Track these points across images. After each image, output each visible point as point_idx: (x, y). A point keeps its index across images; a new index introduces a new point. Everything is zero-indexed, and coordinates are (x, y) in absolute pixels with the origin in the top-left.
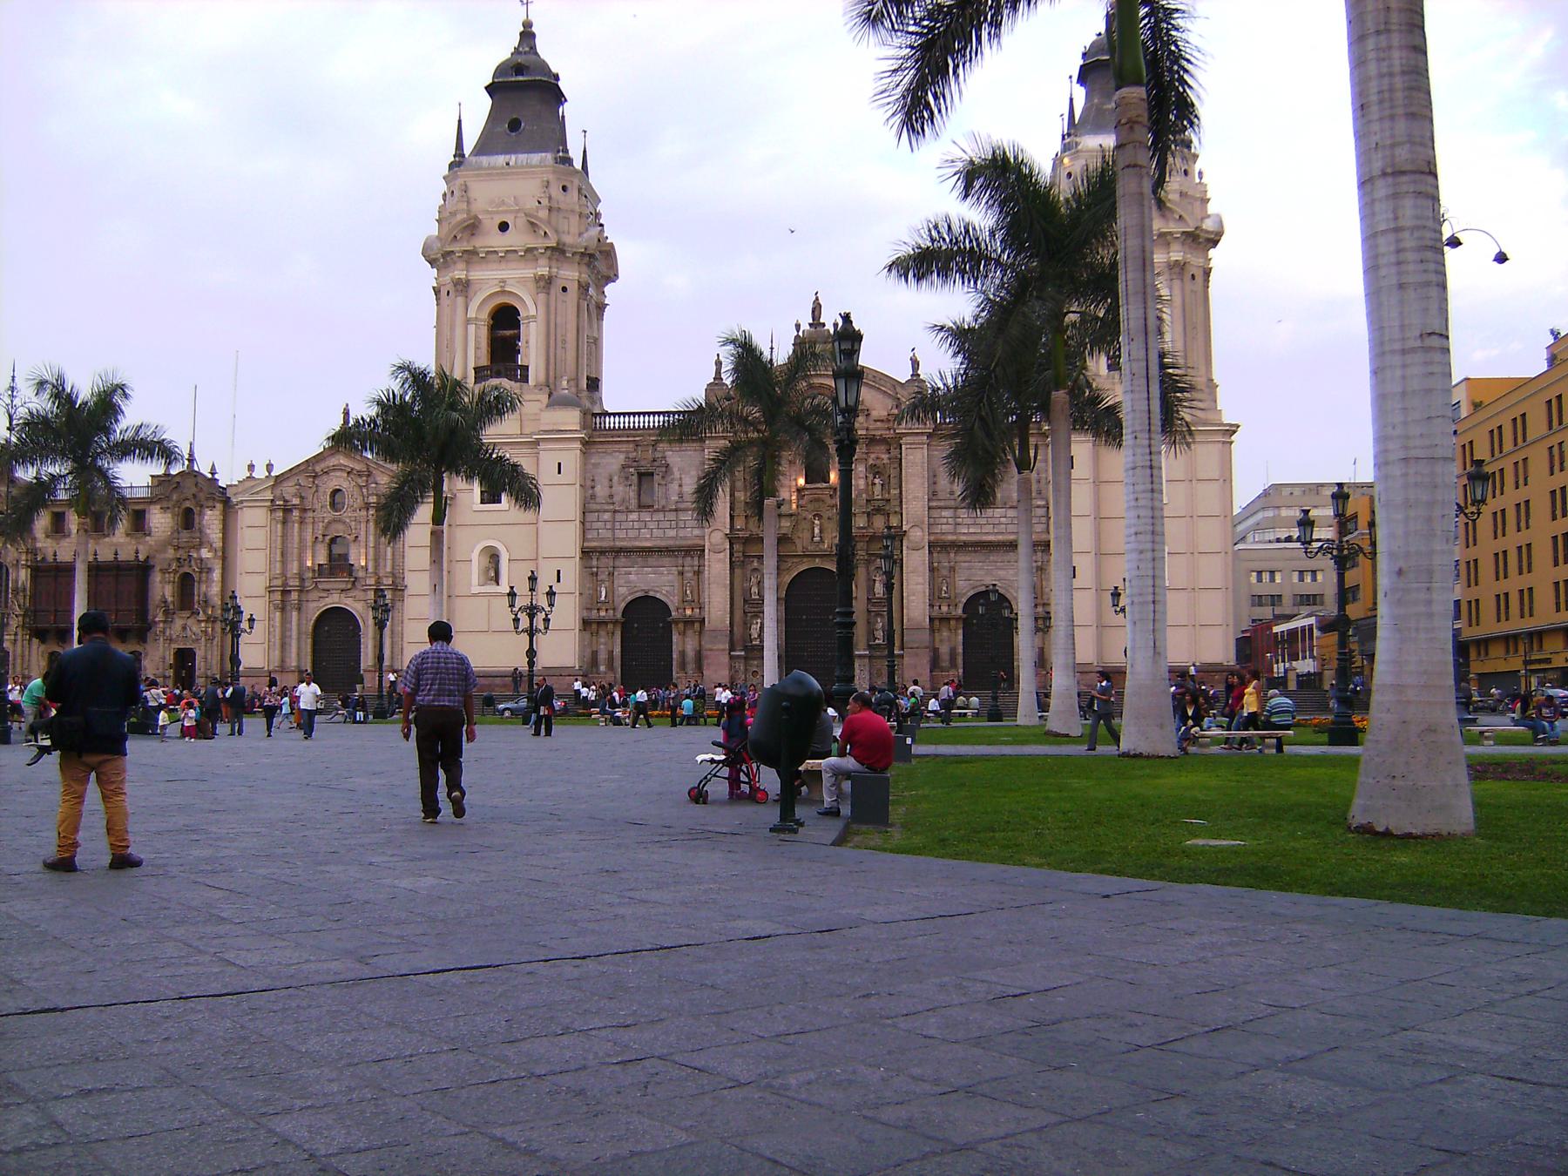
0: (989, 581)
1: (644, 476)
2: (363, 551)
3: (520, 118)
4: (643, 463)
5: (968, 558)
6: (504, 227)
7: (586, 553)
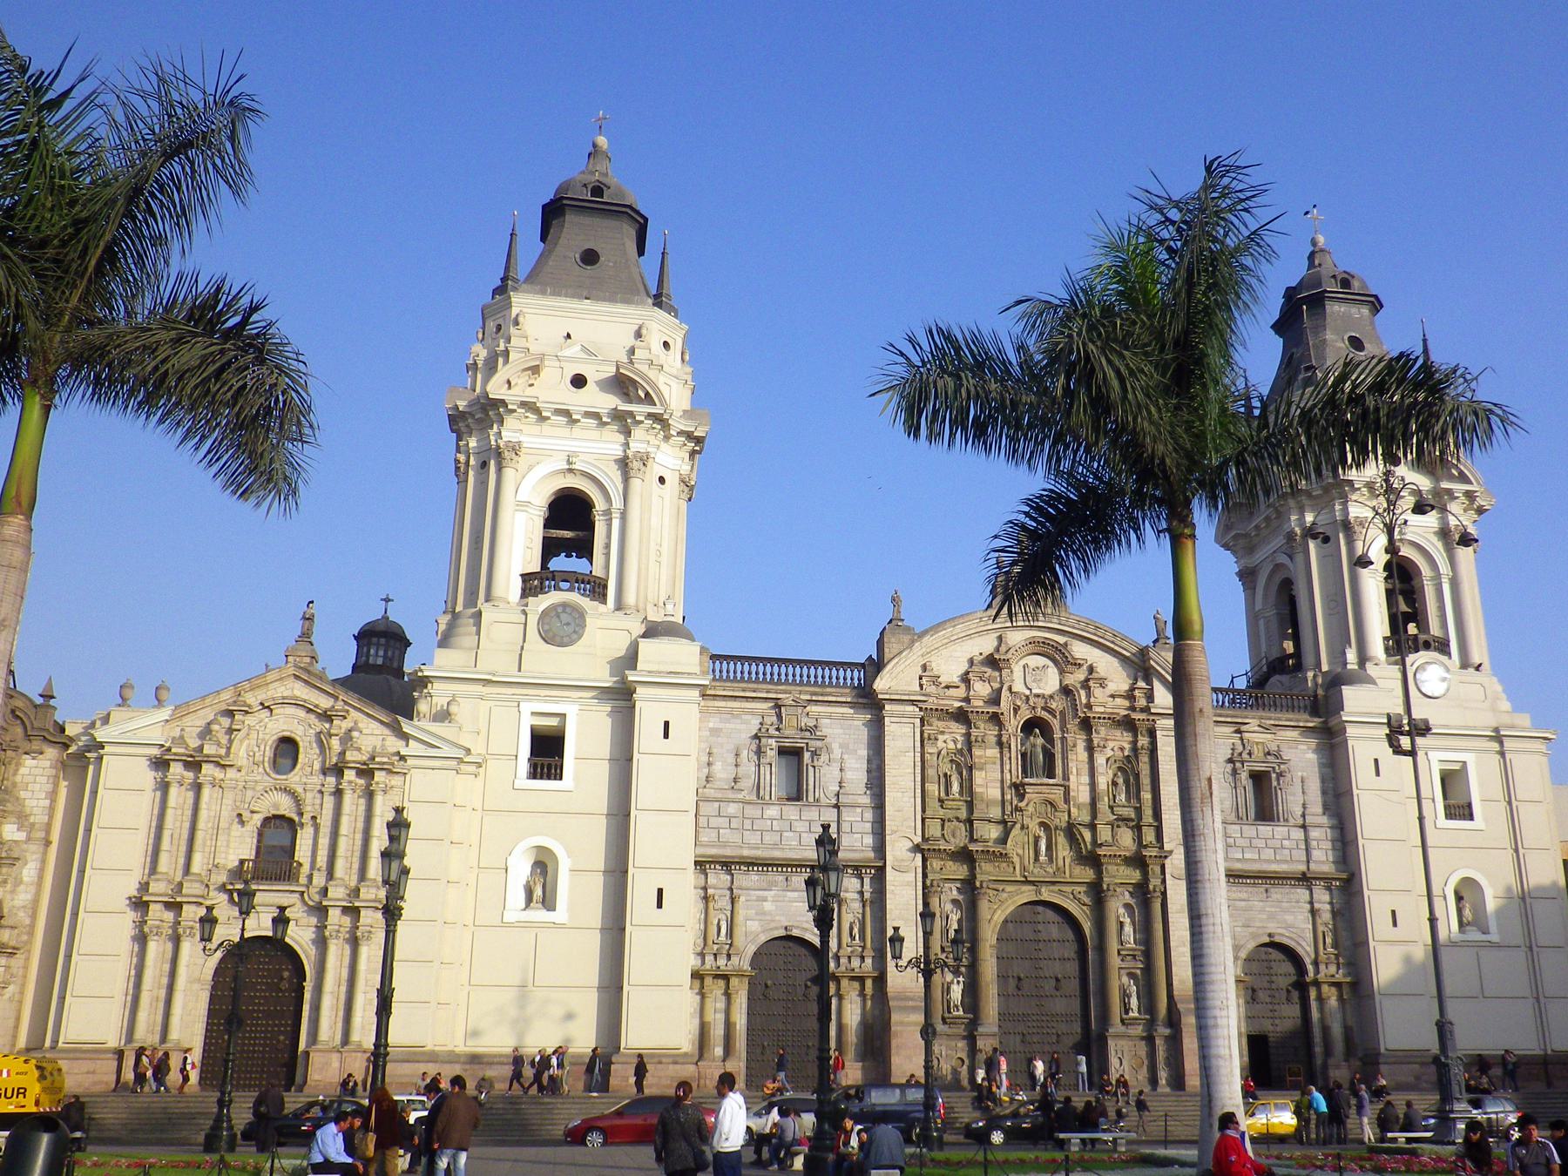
0: (1272, 927)
1: (791, 754)
2: (324, 842)
3: (599, 251)
4: (787, 732)
5: (1244, 896)
6: (579, 381)
7: (701, 865)
